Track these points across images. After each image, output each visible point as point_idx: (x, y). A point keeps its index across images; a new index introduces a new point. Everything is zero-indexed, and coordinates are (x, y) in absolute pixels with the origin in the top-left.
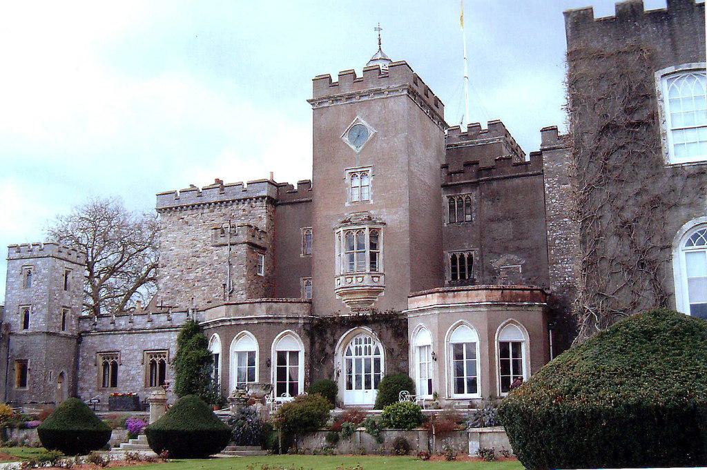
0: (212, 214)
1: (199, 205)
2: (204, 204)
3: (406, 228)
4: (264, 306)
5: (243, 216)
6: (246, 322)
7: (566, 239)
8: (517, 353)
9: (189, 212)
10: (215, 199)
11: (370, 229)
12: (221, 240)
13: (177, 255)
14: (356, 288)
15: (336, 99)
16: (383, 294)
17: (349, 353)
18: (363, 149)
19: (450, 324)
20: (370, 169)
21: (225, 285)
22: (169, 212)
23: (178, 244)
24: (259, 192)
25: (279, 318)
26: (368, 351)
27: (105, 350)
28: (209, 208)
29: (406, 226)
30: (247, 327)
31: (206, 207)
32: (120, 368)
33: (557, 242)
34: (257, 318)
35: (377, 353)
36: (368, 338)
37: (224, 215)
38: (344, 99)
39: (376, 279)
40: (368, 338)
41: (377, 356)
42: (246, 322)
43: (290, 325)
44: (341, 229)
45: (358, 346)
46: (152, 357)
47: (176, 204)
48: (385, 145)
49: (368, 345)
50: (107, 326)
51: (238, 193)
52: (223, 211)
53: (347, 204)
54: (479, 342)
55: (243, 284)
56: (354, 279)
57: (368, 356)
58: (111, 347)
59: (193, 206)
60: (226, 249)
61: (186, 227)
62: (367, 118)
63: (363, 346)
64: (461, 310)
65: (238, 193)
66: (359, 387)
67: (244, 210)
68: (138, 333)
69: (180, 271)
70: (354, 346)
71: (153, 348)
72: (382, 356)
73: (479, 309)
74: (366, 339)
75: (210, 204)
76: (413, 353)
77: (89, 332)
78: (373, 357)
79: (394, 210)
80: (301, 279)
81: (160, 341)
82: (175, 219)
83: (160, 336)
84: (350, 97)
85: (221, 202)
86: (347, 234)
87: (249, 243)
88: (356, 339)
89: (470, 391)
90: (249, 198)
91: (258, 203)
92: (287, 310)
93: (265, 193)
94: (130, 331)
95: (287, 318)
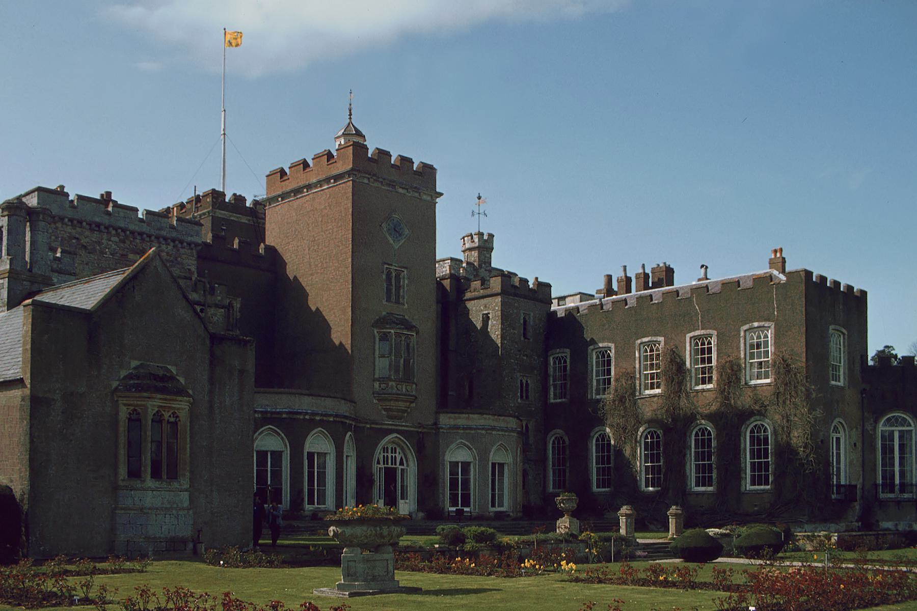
30: (322, 423)
35: (401, 463)
45: (386, 455)
74: (392, 448)
88: (384, 448)
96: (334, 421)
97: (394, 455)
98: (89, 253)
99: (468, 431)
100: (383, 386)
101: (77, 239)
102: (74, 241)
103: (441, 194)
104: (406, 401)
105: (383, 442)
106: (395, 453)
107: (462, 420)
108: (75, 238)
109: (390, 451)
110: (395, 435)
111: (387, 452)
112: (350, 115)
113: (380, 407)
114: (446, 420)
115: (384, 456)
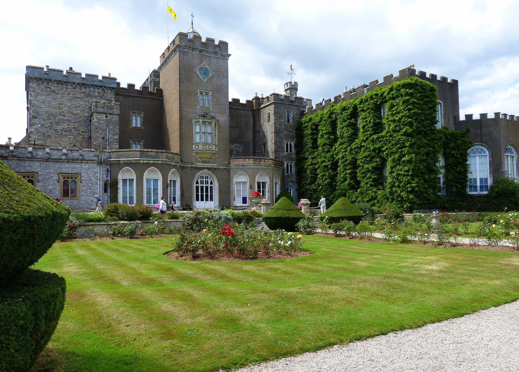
1: (65, 82)
2: (69, 83)
3: (228, 126)
4: (164, 155)
5: (98, 96)
7: (281, 142)
8: (264, 187)
12: (101, 110)
13: (46, 112)
14: (208, 151)
17: (197, 183)
21: (103, 138)
24: (111, 84)
26: (207, 182)
27: (23, 171)
29: (228, 124)
30: (154, 165)
33: (278, 143)
35: (211, 183)
37: (84, 93)
38: (197, 51)
41: (211, 185)
42: (154, 162)
44: (201, 120)
45: (202, 180)
47: (45, 77)
50: (24, 154)
51: (95, 81)
52: (83, 90)
53: (198, 107)
54: (269, 182)
56: (208, 146)
57: (207, 185)
58: (28, 169)
59: (60, 81)
61: (53, 94)
62: (209, 65)
63: (204, 180)
66: (202, 200)
67: (99, 93)
68: (54, 161)
69: (49, 123)
71: (67, 172)
73: (269, 167)
74: (206, 177)
75: (74, 83)
77: (7, 157)
78: (209, 185)
80: (131, 140)
83: (73, 165)
85: (83, 84)
88: (201, 177)
91: (108, 91)
94: (48, 160)
97: (207, 180)
99: (244, 167)
100: (197, 147)
101: (50, 88)
102: (48, 89)
103: (230, 55)
104: (210, 153)
105: (198, 174)
106: (208, 179)
107: (241, 162)
108: (49, 88)
109: (204, 178)
111: (203, 178)
112: (192, 24)
114: (235, 163)
115: (201, 180)
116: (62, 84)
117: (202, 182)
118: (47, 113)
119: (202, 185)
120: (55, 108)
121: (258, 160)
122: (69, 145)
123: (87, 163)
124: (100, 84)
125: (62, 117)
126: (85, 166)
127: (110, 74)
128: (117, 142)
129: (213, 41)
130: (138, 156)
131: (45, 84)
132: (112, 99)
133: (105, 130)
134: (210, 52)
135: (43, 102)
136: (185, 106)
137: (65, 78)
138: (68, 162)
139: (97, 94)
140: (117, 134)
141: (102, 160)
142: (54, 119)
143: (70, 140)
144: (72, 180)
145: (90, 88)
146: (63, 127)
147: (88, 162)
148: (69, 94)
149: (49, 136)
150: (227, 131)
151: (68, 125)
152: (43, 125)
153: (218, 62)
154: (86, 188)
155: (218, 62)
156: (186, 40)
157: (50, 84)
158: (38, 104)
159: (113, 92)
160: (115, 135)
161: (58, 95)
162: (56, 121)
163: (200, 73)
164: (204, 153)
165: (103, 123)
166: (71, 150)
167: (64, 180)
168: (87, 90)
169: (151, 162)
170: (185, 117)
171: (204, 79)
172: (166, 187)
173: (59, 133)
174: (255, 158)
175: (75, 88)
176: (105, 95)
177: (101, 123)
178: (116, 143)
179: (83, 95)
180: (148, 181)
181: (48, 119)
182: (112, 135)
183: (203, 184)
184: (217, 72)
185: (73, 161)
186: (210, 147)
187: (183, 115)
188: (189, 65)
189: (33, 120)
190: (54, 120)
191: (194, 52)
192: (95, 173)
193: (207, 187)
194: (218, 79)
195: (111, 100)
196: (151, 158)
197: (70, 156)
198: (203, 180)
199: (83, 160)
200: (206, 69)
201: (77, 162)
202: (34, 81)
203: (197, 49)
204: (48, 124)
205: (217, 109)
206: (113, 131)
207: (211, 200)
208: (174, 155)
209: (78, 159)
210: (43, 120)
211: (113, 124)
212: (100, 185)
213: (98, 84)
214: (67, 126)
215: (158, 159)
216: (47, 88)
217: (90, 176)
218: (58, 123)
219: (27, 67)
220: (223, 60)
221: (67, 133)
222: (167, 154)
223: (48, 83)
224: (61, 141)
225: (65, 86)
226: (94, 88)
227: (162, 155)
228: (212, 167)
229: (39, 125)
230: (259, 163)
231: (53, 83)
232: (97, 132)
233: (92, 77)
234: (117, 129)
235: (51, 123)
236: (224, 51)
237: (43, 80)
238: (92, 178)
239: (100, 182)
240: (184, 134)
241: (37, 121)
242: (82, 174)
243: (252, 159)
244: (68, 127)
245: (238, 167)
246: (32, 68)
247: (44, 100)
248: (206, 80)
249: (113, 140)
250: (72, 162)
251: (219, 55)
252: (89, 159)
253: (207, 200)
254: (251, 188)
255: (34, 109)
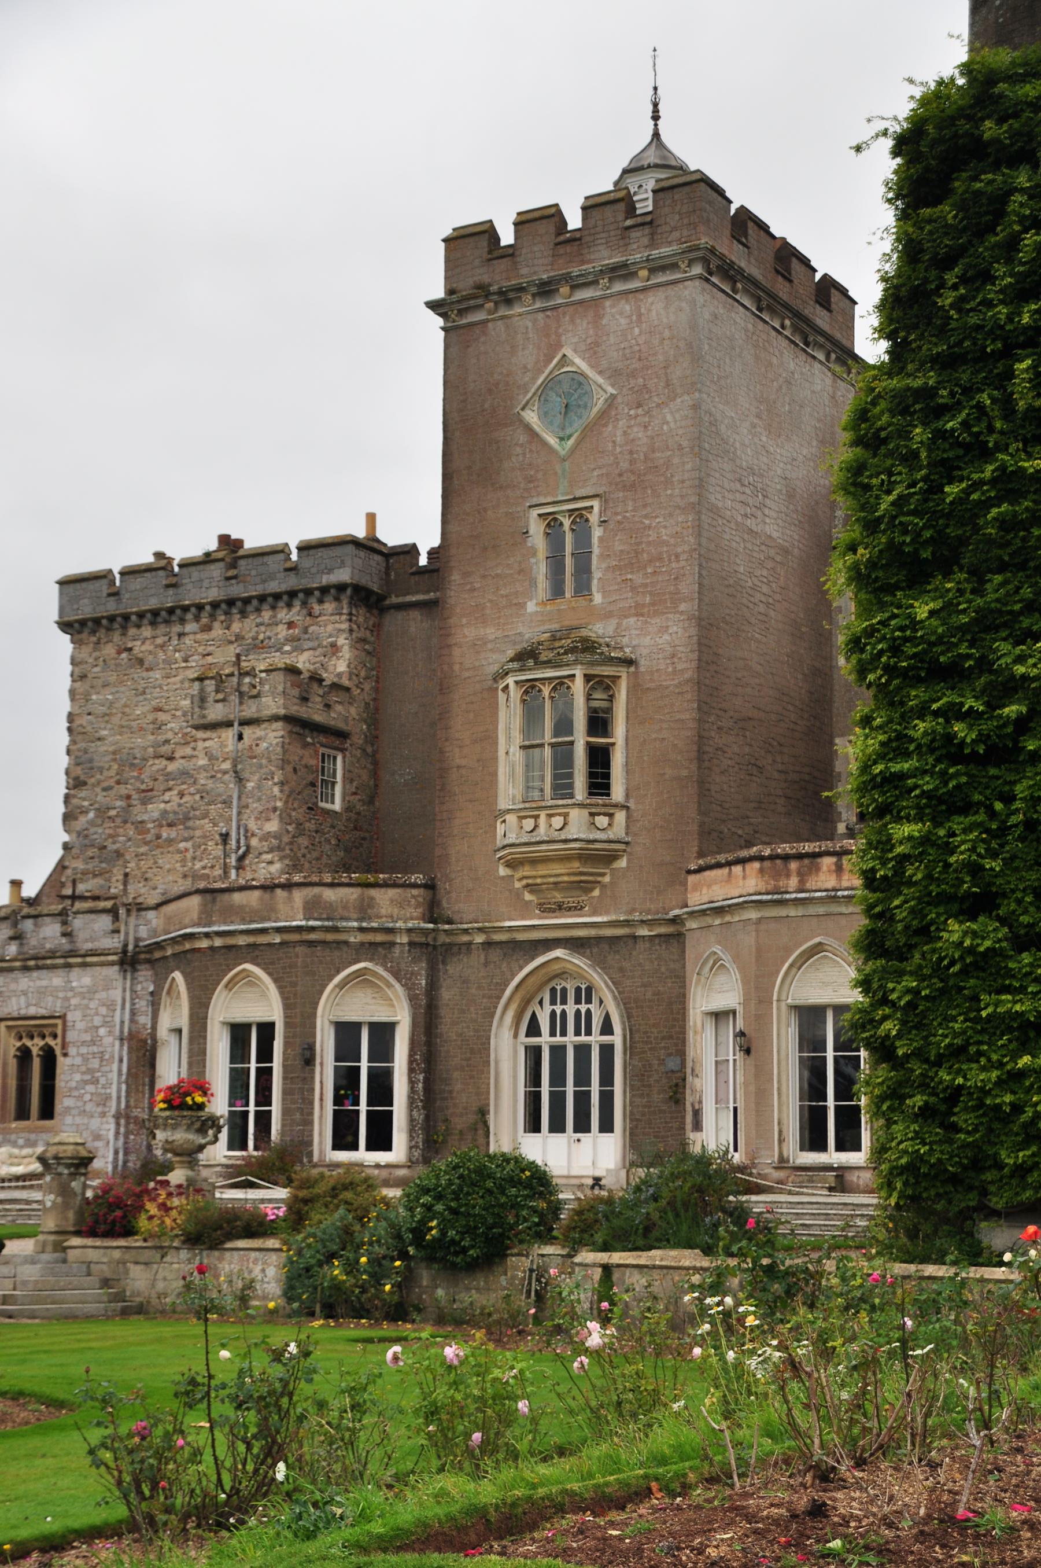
0: (205, 636)
1: (171, 611)
2: (186, 609)
4: (299, 896)
6: (251, 939)
9: (147, 632)
10: (214, 594)
11: (588, 678)
12: (216, 712)
13: (114, 753)
14: (544, 847)
15: (507, 297)
16: (622, 863)
17: (533, 1029)
18: (578, 444)
19: (789, 952)
20: (596, 503)
22: (94, 632)
23: (116, 720)
24: (330, 571)
25: (335, 929)
28: (197, 618)
29: (687, 665)
30: (253, 952)
31: (189, 616)
32: (62, 1064)
34: (278, 930)
35: (607, 1028)
36: (583, 987)
37: (239, 638)
39: (602, 821)
40: (583, 987)
42: (251, 939)
43: (369, 950)
46: (20, 1038)
47: (111, 607)
48: (637, 432)
49: (583, 1007)
55: (277, 836)
56: (542, 820)
59: (155, 613)
60: (229, 735)
61: (138, 673)
62: (593, 351)
64: (821, 910)
65: (272, 577)
66: (557, 1126)
67: (291, 625)
69: (121, 798)
70: (548, 1008)
71: (23, 1012)
72: (617, 1039)
74: (578, 990)
75: (200, 607)
76: (695, 1032)
79: (657, 621)
81: (42, 992)
82: (109, 650)
84: (546, 289)
85: (231, 603)
86: (526, 692)
87: (288, 719)
88: (553, 991)
89: (840, 1147)
90: (301, 591)
92: (364, 909)
93: (343, 576)
95: (361, 930)
96: (283, 944)
98: (147, 670)
101: (130, 649)
102: (124, 655)
106: (589, 1001)
110: (559, 953)
111: (564, 1002)
112: (656, 117)
113: (518, 885)
115: (553, 1014)
116: (167, 622)
117: (584, 1025)
118: (115, 760)
119: (558, 1039)
120: (141, 729)
121: (794, 865)
122: (180, 881)
123: (84, 965)
124: (291, 582)
125: (164, 762)
126: (79, 980)
127: (371, 519)
128: (271, 851)
129: (553, 215)
130: (195, 916)
131: (116, 637)
132: (341, 641)
133: (227, 803)
134: (591, 278)
135: (106, 715)
136: (464, 621)
137: (171, 591)
138: (26, 969)
139: (282, 631)
140: (275, 809)
141: (131, 947)
142: (137, 778)
143: (184, 861)
144: (42, 1043)
145: (258, 610)
146: (162, 806)
147: (89, 959)
148: (186, 661)
149: (119, 854)
150: (685, 710)
151: (181, 795)
152: (102, 812)
153: (640, 316)
154: (78, 1077)
155: (640, 316)
156: (477, 262)
157: (132, 631)
158: (89, 728)
159: (345, 603)
160: (263, 816)
161: (151, 674)
162: (143, 787)
163: (544, 415)
164: (534, 862)
165: (225, 772)
166: (36, 917)
167: (18, 1044)
168: (245, 626)
169: (242, 941)
170: (466, 674)
171: (562, 439)
172: (298, 1062)
173: (149, 837)
174: (772, 858)
175: (208, 628)
176: (311, 629)
177: (219, 771)
178: (269, 857)
179: (232, 647)
180: (239, 1033)
181: (118, 783)
182: (257, 819)
183: (564, 1033)
184: (633, 375)
185: (40, 963)
186: (557, 822)
187: (456, 667)
188: (490, 391)
189: (74, 796)
190: (138, 785)
191: (518, 309)
192: (111, 1006)
193: (583, 1052)
194: (637, 416)
195: (333, 645)
196: (243, 921)
197: (33, 942)
198: (564, 1012)
199: (72, 953)
200: (579, 380)
201: (54, 967)
202: (84, 636)
203: (521, 289)
204: (118, 803)
205: (633, 589)
206: (259, 799)
207: (607, 1126)
208: (373, 892)
209: (52, 954)
210: (105, 789)
211: (261, 766)
212: (121, 1061)
213: (283, 588)
214: (176, 799)
215: (269, 920)
216: (119, 653)
217: (97, 1021)
218: (147, 795)
219: (63, 583)
220: (671, 291)
221: (173, 833)
222: (317, 890)
223: (124, 628)
224: (155, 870)
225: (177, 629)
226: (273, 608)
227: (290, 899)
228: (593, 932)
229: (91, 815)
230: (802, 882)
231: (139, 626)
232: (205, 816)
233: (259, 560)
234: (276, 790)
235: (129, 797)
236: (676, 234)
237: (104, 622)
238: (102, 1031)
239: (122, 1045)
240: (459, 767)
241: (84, 799)
242: (69, 1017)
243: (757, 865)
244: (180, 805)
245: (709, 920)
246: (72, 586)
247: (112, 704)
248: (571, 442)
249: (261, 840)
250: (38, 968)
251: (644, 273)
252: (89, 946)
253: (582, 1125)
254: (748, 1052)
255: (79, 750)
